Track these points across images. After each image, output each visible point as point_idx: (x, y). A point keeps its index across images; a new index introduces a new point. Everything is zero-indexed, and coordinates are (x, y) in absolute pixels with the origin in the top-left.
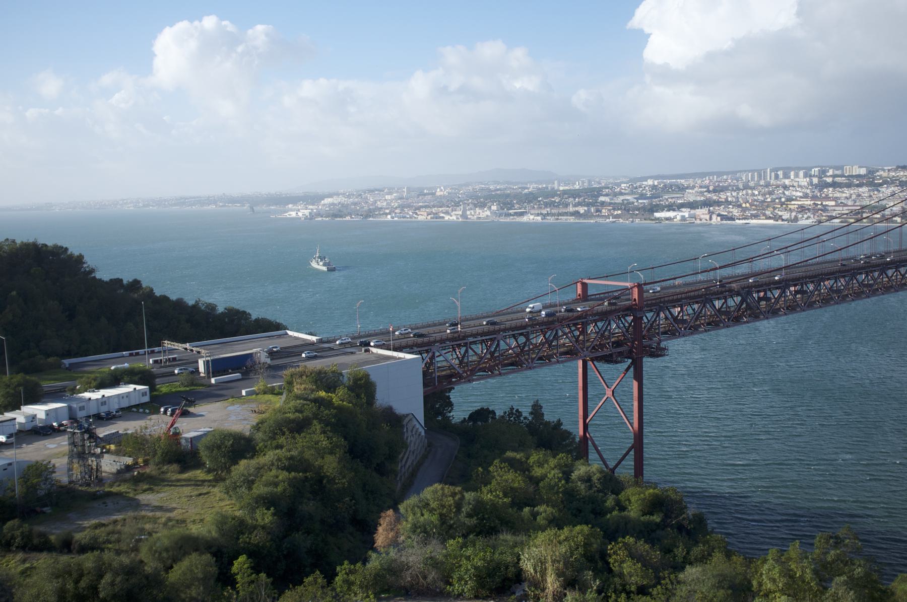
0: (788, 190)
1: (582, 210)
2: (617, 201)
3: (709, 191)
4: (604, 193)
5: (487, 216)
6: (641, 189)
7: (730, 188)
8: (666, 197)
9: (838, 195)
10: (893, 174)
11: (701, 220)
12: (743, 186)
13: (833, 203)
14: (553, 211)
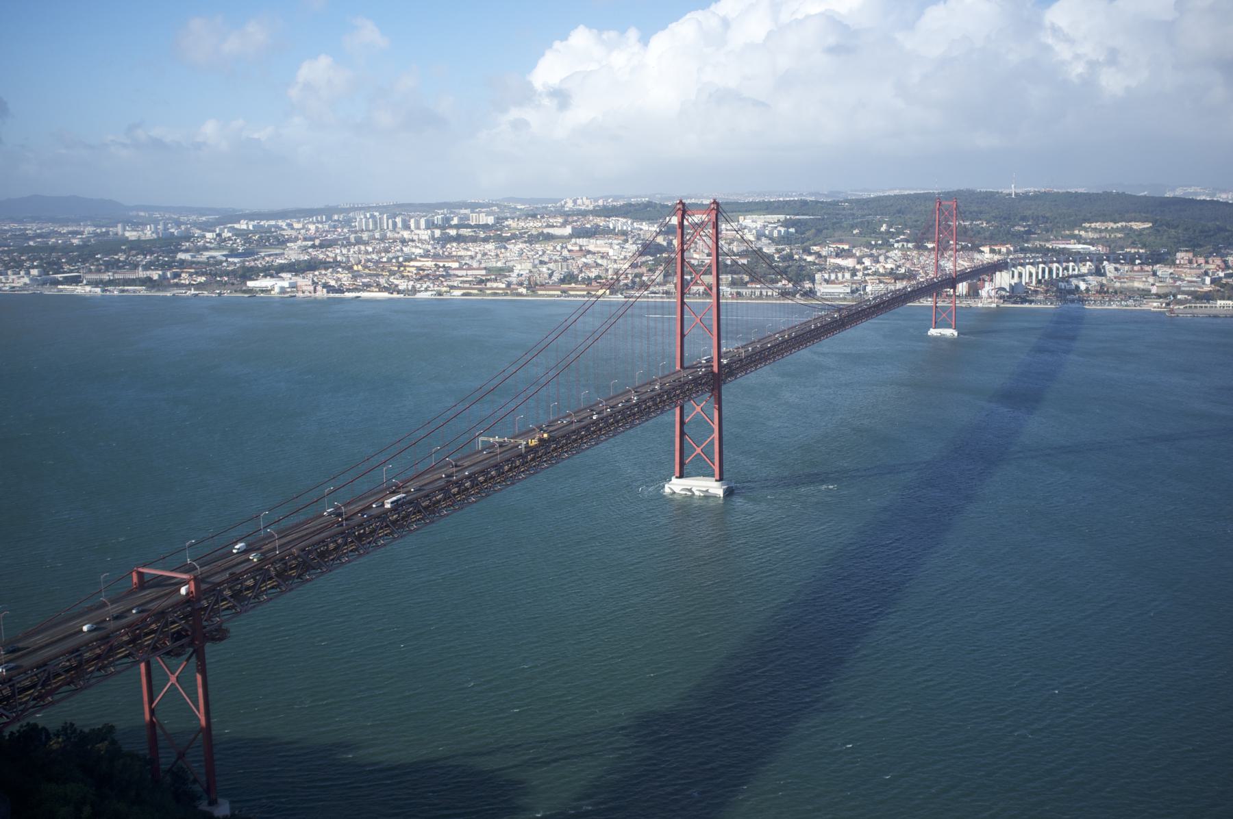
0: (406, 246)
1: (155, 275)
2: (199, 260)
3: (313, 246)
4: (184, 248)
5: (25, 284)
6: (231, 242)
7: (340, 243)
8: (263, 254)
9: (462, 253)
10: (523, 224)
11: (303, 292)
12: (355, 240)
13: (455, 265)
14: (117, 276)
